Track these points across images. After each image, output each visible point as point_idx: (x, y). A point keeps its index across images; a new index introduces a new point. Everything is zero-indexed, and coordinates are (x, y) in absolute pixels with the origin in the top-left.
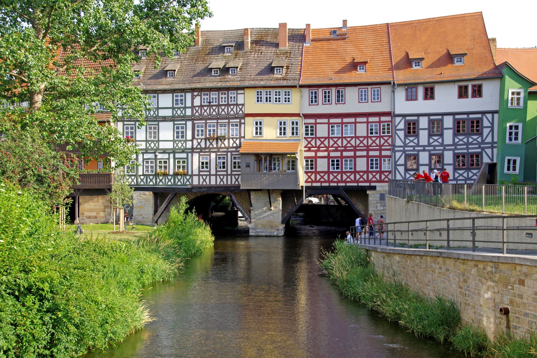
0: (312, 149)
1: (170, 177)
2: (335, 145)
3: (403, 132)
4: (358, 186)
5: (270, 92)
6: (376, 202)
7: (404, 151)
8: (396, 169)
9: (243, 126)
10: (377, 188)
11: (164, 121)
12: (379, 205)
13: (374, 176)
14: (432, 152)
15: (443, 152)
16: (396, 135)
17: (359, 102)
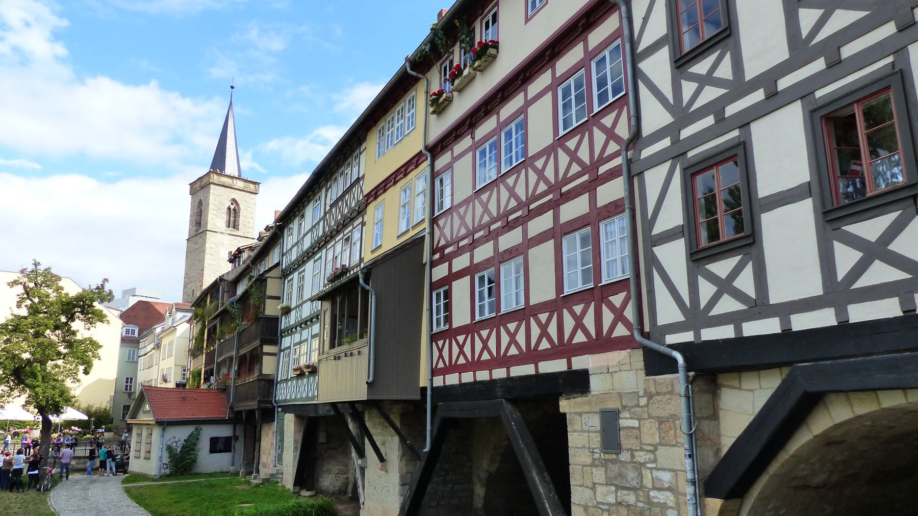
0: (447, 251)
1: (305, 379)
2: (486, 219)
3: (663, 56)
4: (539, 378)
5: (393, 118)
6: (589, 461)
7: (676, 154)
8: (653, 261)
9: (364, 228)
10: (596, 384)
11: (309, 258)
12: (599, 475)
13: (579, 324)
14: (819, 94)
15: (901, 52)
16: (641, 85)
17: (527, 20)
